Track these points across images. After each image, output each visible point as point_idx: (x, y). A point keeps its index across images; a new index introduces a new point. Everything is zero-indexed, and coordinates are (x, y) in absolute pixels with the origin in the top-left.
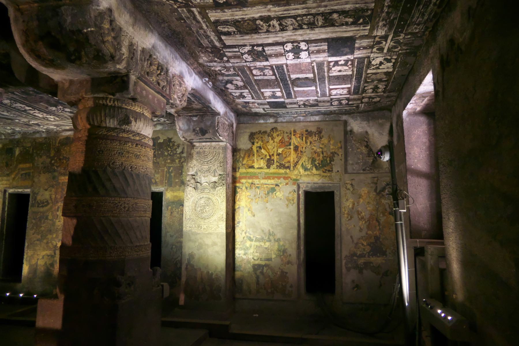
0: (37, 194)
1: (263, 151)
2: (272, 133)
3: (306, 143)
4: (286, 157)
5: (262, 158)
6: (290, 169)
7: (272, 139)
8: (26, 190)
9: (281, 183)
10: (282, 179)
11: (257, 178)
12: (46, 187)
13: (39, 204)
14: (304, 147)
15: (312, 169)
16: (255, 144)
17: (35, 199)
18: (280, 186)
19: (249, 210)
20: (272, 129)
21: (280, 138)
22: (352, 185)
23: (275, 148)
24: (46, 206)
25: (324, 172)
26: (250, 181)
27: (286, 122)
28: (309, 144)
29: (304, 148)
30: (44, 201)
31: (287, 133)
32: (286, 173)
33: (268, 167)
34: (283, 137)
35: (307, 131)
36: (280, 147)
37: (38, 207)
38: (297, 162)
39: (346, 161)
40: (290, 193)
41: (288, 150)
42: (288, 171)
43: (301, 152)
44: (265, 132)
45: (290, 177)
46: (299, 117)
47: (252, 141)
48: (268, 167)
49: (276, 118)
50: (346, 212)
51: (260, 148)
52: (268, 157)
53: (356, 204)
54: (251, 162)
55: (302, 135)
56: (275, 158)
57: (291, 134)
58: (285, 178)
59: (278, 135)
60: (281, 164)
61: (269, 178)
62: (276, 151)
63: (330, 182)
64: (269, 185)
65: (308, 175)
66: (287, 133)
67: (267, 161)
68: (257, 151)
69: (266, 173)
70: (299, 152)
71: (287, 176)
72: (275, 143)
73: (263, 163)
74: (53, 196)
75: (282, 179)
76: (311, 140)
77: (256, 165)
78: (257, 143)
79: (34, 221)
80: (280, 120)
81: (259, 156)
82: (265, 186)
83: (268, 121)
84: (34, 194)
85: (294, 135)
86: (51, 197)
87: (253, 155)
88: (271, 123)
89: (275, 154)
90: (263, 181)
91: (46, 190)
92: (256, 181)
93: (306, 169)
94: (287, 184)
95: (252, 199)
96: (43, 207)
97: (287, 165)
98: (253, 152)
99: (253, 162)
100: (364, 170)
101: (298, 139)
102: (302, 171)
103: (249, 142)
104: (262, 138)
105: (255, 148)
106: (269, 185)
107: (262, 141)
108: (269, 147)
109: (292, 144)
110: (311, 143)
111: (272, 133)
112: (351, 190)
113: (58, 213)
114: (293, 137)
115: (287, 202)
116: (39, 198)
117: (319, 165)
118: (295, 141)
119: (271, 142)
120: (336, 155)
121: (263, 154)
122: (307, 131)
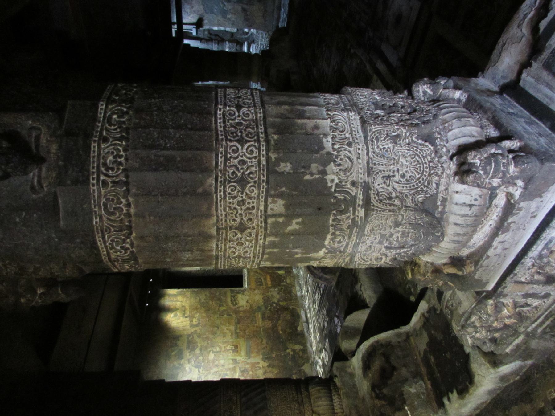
0: (243, 294)
8: (246, 283)
12: (250, 301)
13: (234, 296)
17: (238, 293)
24: (232, 303)
30: (237, 302)
37: (231, 296)
74: (241, 309)
79: (218, 294)
84: (243, 292)
86: (240, 307)
91: (247, 302)
96: (231, 300)
113: (225, 315)
116: (240, 296)
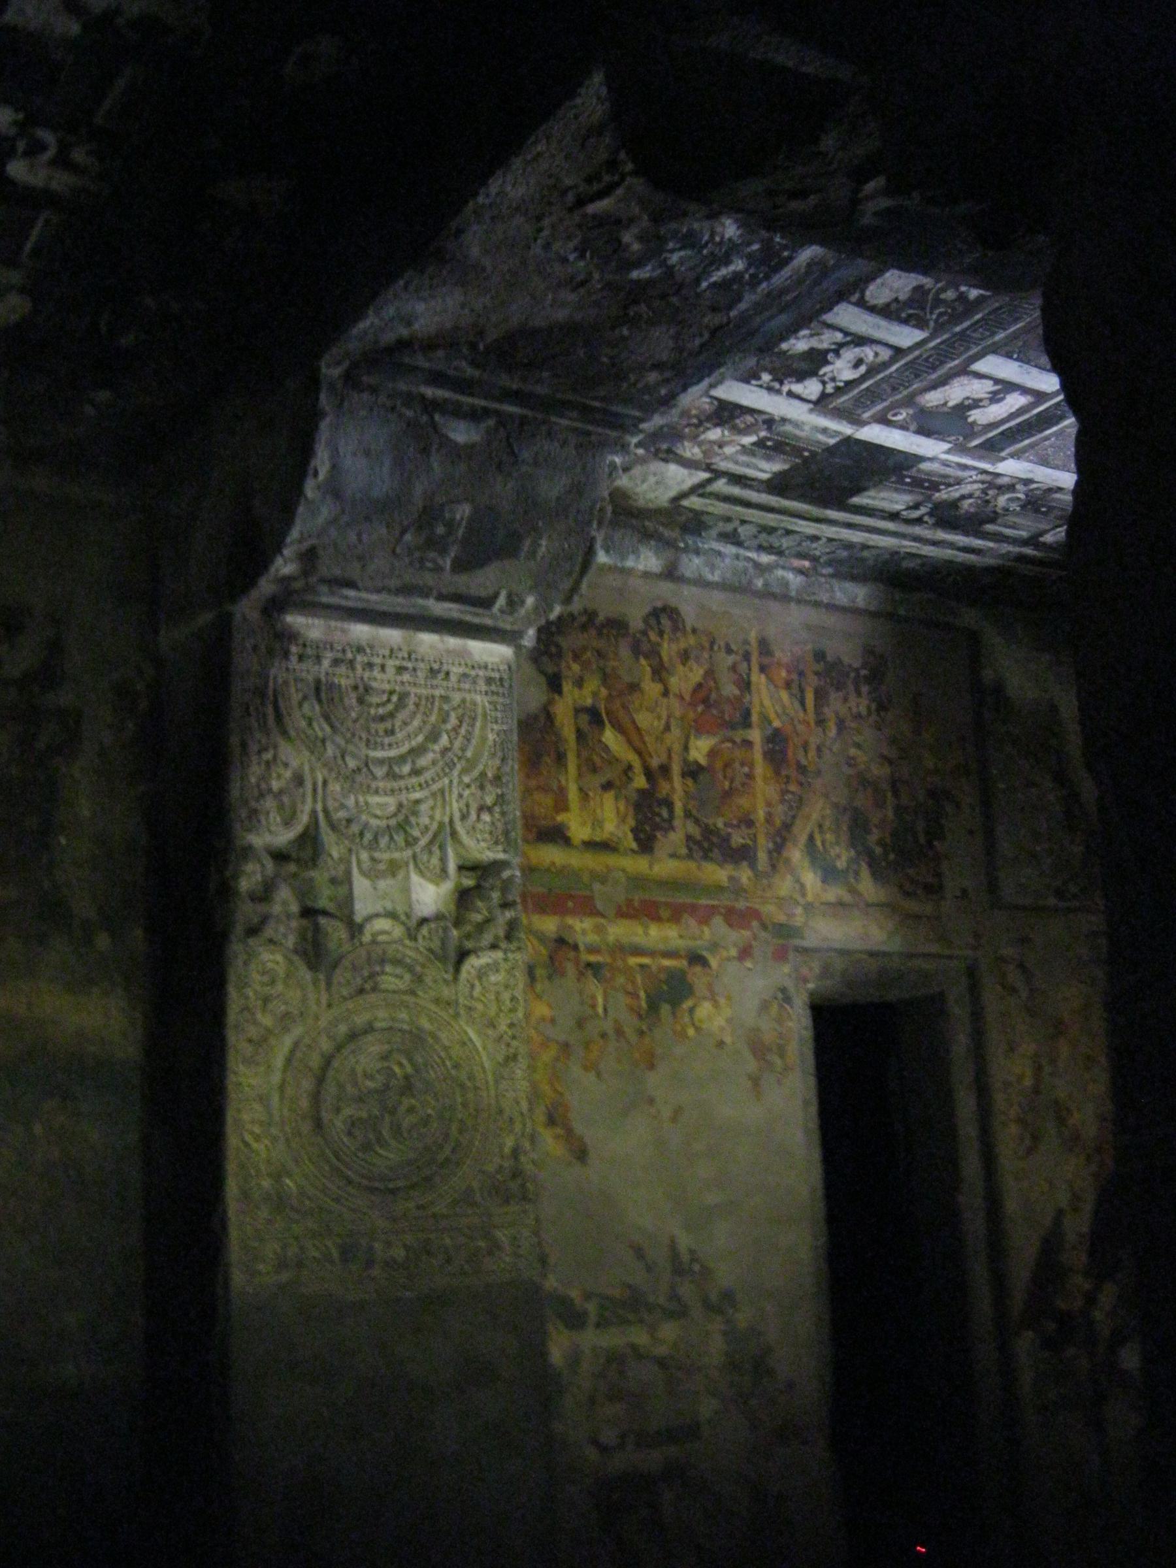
1: (610, 736)
2: (653, 636)
3: (821, 722)
4: (728, 794)
5: (608, 786)
6: (753, 865)
7: (660, 672)
9: (714, 946)
10: (718, 920)
11: (587, 907)
14: (814, 741)
15: (857, 873)
16: (567, 687)
18: (714, 962)
19: (551, 1121)
20: (656, 613)
21: (696, 674)
22: (1021, 966)
23: (676, 732)
25: (907, 894)
26: (549, 925)
27: (723, 586)
28: (833, 732)
29: (812, 753)
31: (729, 651)
32: (738, 890)
33: (646, 844)
34: (710, 673)
35: (820, 656)
36: (700, 728)
38: (787, 826)
39: (990, 848)
40: (765, 1006)
41: (739, 754)
42: (745, 875)
43: (802, 769)
44: (617, 625)
45: (756, 914)
46: (780, 573)
47: (551, 669)
48: (646, 844)
49: (669, 553)
50: (1013, 1112)
51: (594, 716)
52: (640, 782)
53: (1047, 1069)
54: (548, 800)
55: (801, 674)
56: (677, 788)
57: (747, 657)
58: (736, 918)
59: (685, 656)
60: (708, 832)
61: (649, 912)
62: (677, 747)
63: (934, 948)
64: (652, 954)
65: (841, 904)
66: (729, 651)
67: (638, 807)
68: (580, 735)
69: (638, 882)
70: (792, 772)
71: (741, 905)
72: (675, 703)
73: (611, 817)
75: (718, 920)
76: (843, 711)
77: (579, 831)
78: (579, 683)
80: (692, 565)
81: (594, 770)
82: (633, 961)
83: (630, 563)
85: (763, 669)
87: (560, 758)
88: (646, 575)
89: (676, 769)
90: (620, 931)
92: (582, 928)
93: (829, 874)
94: (745, 953)
95: (566, 1047)
97: (737, 839)
98: (559, 739)
99: (562, 805)
100: (1060, 894)
101: (784, 695)
102: (810, 878)
103: (529, 669)
104: (600, 654)
105: (563, 711)
106: (652, 954)
107: (605, 678)
108: (644, 719)
109: (755, 718)
110: (841, 724)
111: (653, 636)
112: (1024, 994)
114: (758, 679)
115: (752, 1065)
117: (886, 853)
118: (767, 703)
119: (652, 689)
120: (949, 808)
121: (613, 760)
122: (820, 656)
